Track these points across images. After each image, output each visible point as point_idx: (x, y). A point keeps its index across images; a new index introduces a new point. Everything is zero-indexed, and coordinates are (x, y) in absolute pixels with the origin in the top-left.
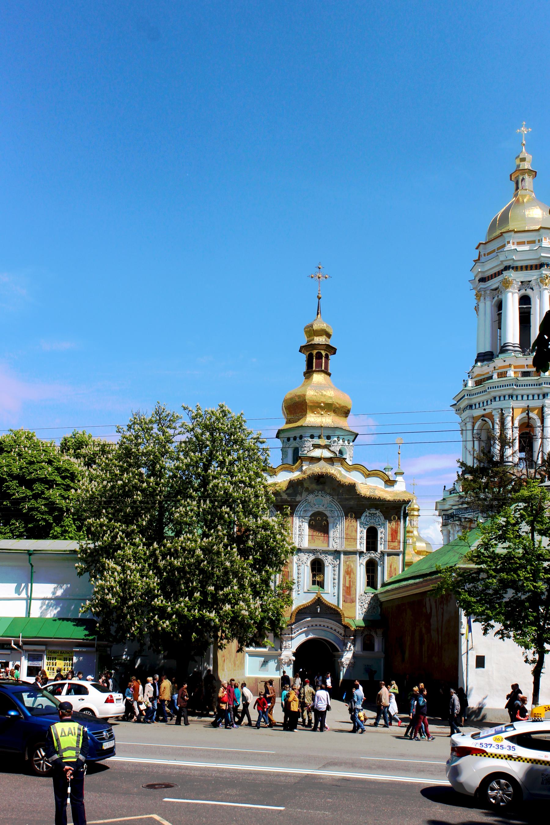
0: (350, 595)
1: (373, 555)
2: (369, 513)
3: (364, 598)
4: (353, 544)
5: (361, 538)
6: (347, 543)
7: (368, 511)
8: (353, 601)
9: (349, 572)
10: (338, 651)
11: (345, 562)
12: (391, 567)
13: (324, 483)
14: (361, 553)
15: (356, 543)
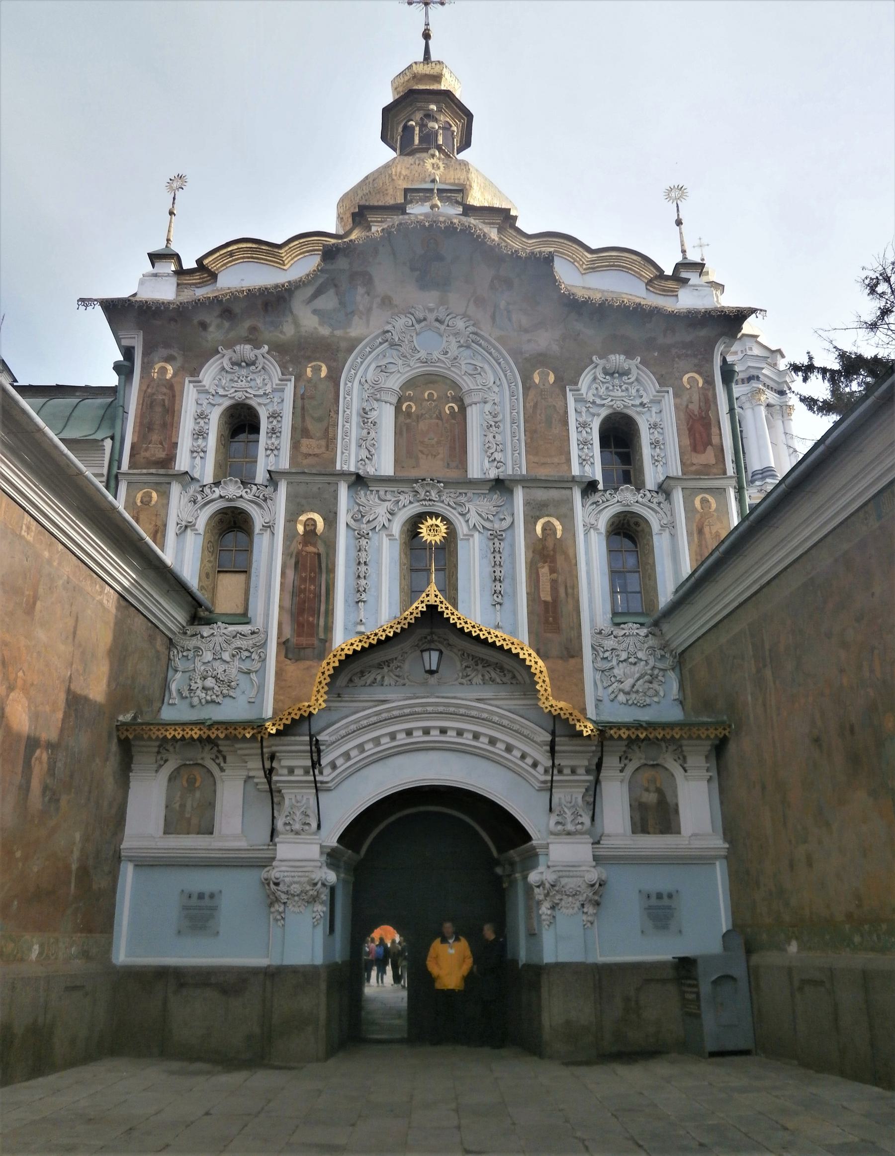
0: (557, 629)
1: (626, 498)
2: (606, 372)
3: (610, 643)
4: (556, 460)
5: (584, 443)
6: (536, 459)
7: (601, 362)
8: (572, 652)
9: (550, 555)
10: (527, 837)
11: (530, 521)
12: (700, 531)
13: (443, 284)
14: (590, 487)
15: (569, 460)
